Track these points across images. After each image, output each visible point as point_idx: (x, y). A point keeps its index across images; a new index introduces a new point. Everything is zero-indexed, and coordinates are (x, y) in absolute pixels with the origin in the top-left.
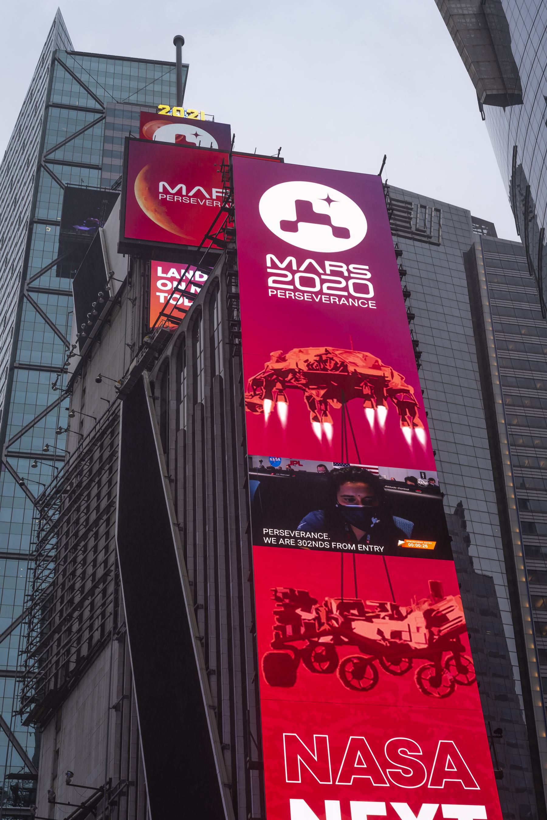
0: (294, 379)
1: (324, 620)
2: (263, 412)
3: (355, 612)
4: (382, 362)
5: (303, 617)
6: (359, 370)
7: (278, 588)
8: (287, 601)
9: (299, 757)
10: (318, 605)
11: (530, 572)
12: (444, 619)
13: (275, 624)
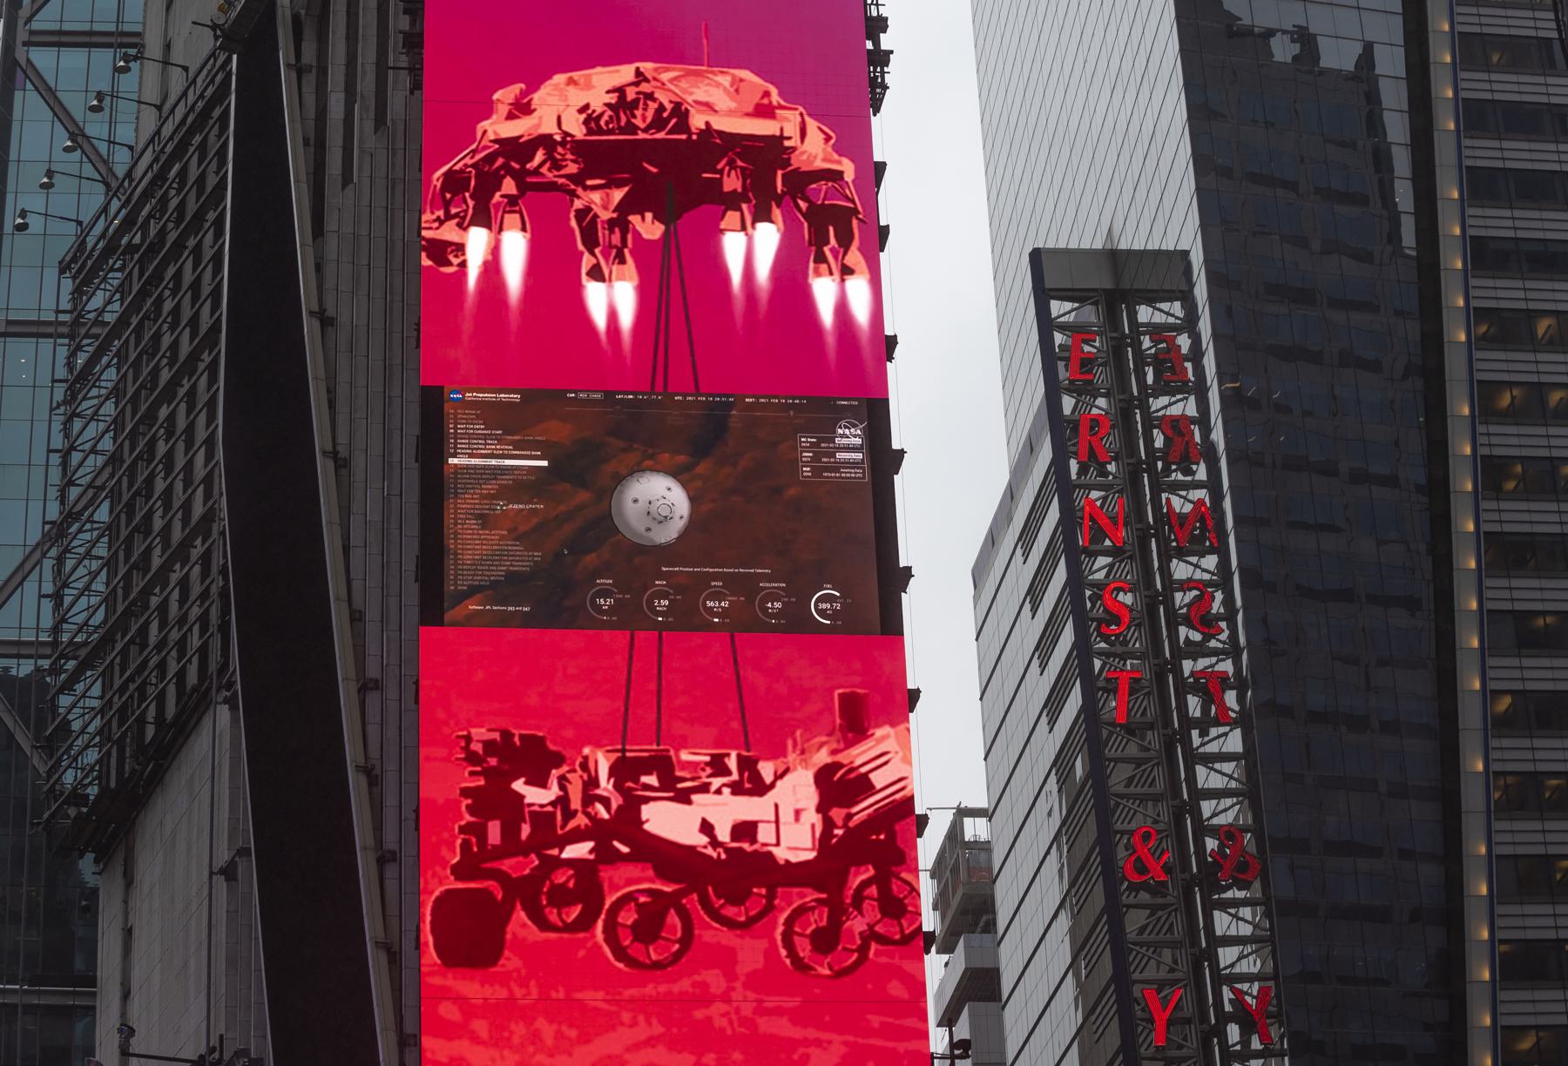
0: (548, 165)
1: (576, 803)
2: (463, 264)
3: (652, 780)
4: (780, 94)
5: (527, 801)
6: (719, 124)
7: (473, 731)
8: (493, 761)
10: (566, 768)
11: (1475, 315)
12: (863, 786)
13: (462, 818)
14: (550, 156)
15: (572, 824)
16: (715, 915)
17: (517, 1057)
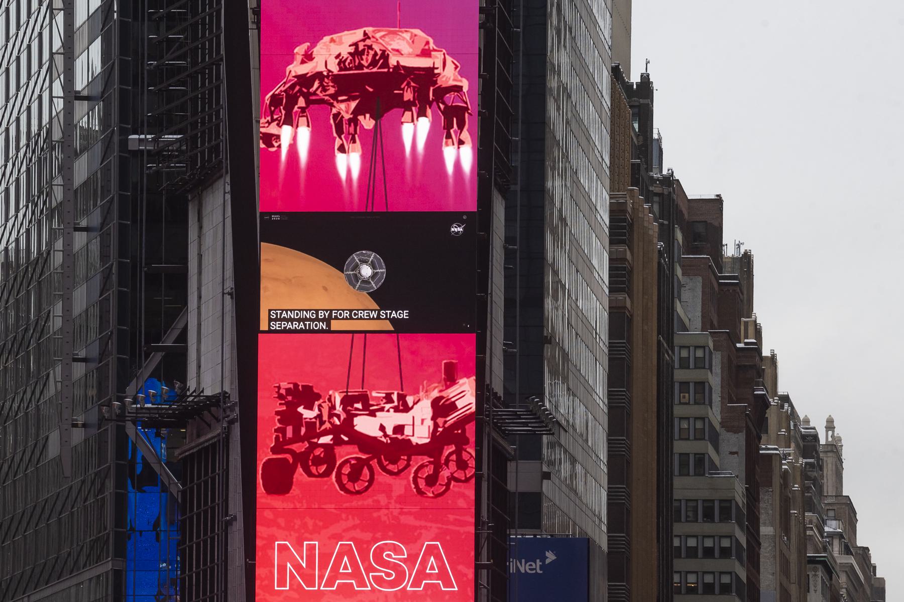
1: (325, 418)
2: (279, 146)
3: (359, 406)
4: (434, 43)
8: (290, 398)
9: (289, 565)
10: (321, 401)
12: (453, 407)
14: (321, 85)
15: (323, 428)
16: (384, 469)
17: (297, 535)
